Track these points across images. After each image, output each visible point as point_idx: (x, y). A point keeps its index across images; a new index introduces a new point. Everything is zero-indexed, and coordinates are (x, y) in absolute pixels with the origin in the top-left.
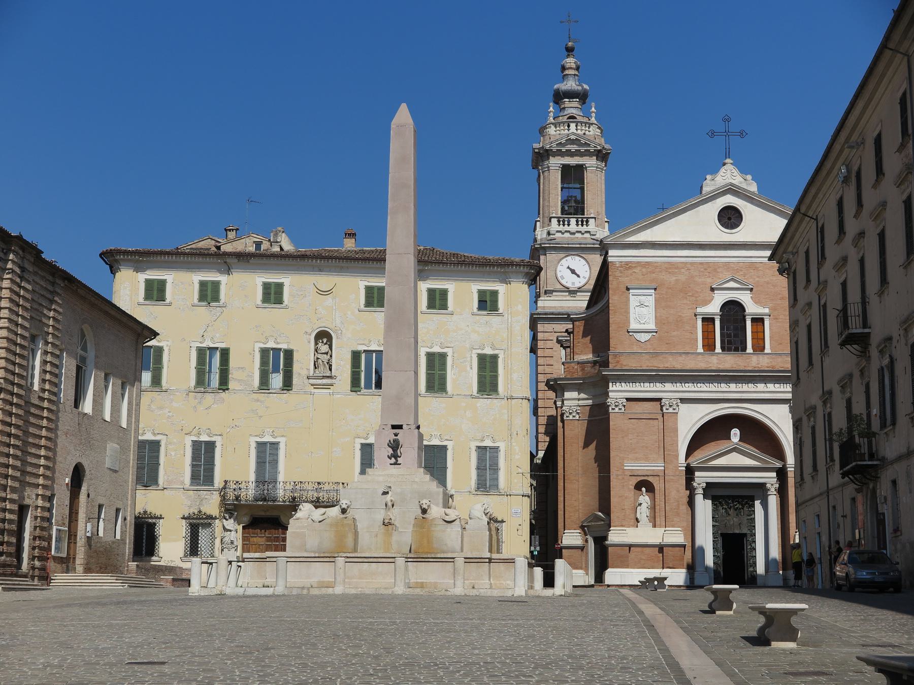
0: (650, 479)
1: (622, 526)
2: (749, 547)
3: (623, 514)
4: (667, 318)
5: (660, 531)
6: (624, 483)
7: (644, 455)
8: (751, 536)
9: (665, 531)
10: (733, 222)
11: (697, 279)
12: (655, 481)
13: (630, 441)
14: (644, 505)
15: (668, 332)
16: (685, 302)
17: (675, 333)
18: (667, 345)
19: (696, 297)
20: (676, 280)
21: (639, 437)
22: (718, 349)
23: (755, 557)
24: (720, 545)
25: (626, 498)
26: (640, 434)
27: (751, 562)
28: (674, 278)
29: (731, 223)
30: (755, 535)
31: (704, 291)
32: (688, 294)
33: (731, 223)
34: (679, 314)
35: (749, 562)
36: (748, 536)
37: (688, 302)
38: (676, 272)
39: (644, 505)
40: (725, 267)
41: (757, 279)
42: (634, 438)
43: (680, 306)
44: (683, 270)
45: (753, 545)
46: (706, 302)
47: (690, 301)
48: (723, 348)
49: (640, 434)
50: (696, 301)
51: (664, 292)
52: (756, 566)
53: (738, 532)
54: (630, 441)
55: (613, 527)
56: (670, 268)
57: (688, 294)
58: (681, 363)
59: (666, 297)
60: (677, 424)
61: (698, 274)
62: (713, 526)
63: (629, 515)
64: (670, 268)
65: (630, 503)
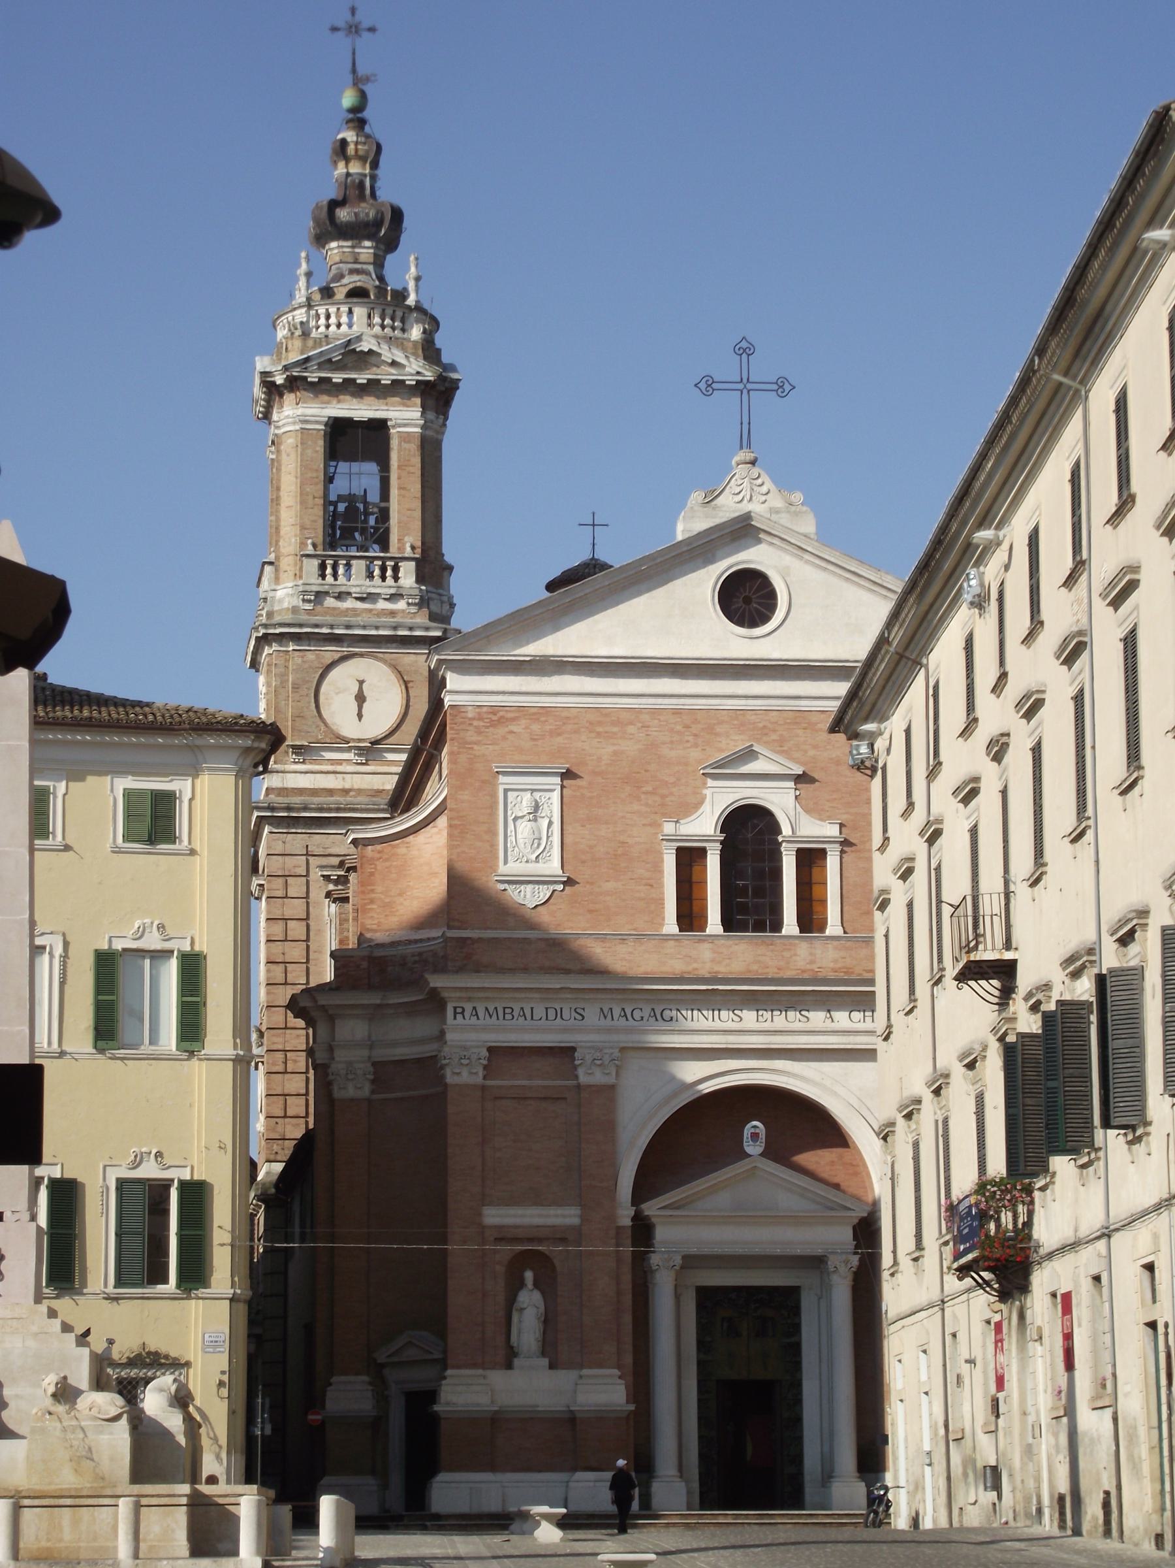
4: (591, 847)
11: (665, 751)
15: (592, 884)
16: (636, 807)
17: (610, 886)
19: (663, 797)
20: (615, 753)
28: (610, 749)
32: (644, 789)
34: (622, 838)
38: (615, 733)
40: (736, 722)
41: (812, 753)
43: (623, 817)
44: (631, 729)
47: (647, 805)
56: (600, 723)
57: (644, 789)
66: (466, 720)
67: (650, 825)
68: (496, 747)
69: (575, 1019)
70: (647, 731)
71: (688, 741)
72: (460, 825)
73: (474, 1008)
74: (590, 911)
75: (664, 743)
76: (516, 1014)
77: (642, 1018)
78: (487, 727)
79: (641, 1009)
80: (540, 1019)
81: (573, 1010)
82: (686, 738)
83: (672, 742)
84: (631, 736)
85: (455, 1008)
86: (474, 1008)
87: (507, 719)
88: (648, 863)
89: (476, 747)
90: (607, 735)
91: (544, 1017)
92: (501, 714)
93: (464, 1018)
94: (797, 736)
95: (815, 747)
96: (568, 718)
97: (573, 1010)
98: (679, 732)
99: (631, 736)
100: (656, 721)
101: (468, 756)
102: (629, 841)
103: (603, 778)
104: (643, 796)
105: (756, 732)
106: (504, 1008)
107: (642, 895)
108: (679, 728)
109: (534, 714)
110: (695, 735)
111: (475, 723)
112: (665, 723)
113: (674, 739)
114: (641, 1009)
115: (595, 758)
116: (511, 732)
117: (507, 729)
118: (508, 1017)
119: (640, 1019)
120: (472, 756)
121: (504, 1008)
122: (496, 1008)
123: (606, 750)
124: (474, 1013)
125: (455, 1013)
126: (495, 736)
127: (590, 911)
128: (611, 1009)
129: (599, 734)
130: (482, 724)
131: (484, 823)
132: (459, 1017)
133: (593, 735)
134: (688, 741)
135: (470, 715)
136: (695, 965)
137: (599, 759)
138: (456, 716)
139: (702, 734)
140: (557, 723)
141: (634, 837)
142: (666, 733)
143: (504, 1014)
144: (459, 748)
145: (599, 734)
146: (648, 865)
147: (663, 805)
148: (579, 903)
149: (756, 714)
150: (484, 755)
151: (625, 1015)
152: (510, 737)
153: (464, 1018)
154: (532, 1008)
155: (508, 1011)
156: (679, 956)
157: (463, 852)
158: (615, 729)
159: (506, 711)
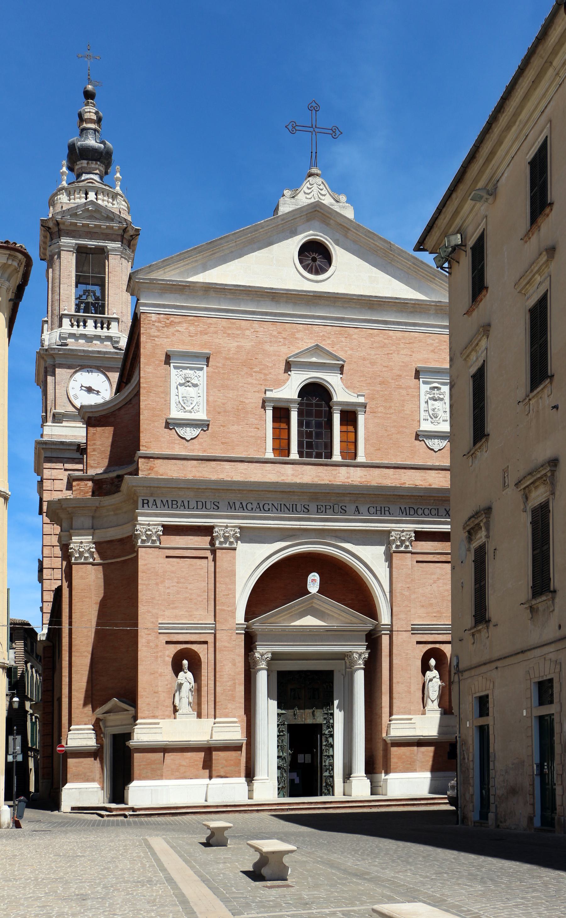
0: (194, 647)
1: (154, 717)
2: (324, 743)
3: (156, 699)
4: (224, 404)
5: (207, 723)
6: (157, 652)
7: (187, 611)
8: (328, 727)
9: (214, 724)
10: (319, 265)
11: (267, 347)
12: (202, 649)
13: (168, 591)
14: (186, 687)
15: (224, 426)
16: (250, 380)
17: (235, 428)
18: (222, 446)
19: (265, 375)
20: (238, 347)
21: (180, 585)
22: (294, 455)
24: (286, 743)
25: (161, 675)
26: (182, 580)
28: (235, 344)
29: (316, 265)
30: (333, 727)
31: (277, 366)
32: (254, 370)
33: (316, 265)
34: (241, 399)
36: (324, 728)
37: (255, 382)
38: (238, 335)
39: (186, 687)
40: (307, 332)
41: (350, 352)
42: (173, 586)
43: (243, 386)
44: (248, 332)
45: (330, 740)
46: (279, 384)
47: (256, 379)
48: (301, 453)
49: (182, 580)
50: (265, 380)
51: (220, 365)
53: (311, 723)
54: (168, 591)
55: (141, 718)
56: (229, 328)
57: (254, 370)
58: (241, 473)
59: (222, 372)
60: (234, 565)
61: (268, 340)
62: (278, 714)
63: (164, 701)
64: (229, 328)
65: (166, 683)
67: (258, 392)
69: (214, 508)
70: (256, 334)
71: (280, 342)
75: (266, 342)
79: (252, 503)
80: (193, 508)
81: (212, 503)
82: (279, 340)
83: (271, 342)
88: (257, 415)
91: (196, 507)
94: (342, 342)
95: (352, 349)
97: (212, 503)
98: (274, 336)
99: (247, 337)
100: (262, 328)
102: (247, 401)
103: (231, 362)
104: (254, 374)
105: (318, 338)
107: (253, 434)
108: (275, 333)
110: (284, 338)
114: (252, 503)
115: (226, 349)
123: (233, 344)
128: (234, 503)
129: (229, 334)
134: (280, 342)
136: (283, 478)
137: (229, 350)
141: (248, 399)
142: (268, 336)
146: (256, 416)
147: (265, 380)
148: (217, 438)
149: (319, 327)
151: (243, 507)
154: (188, 501)
156: (273, 472)
158: (239, 332)
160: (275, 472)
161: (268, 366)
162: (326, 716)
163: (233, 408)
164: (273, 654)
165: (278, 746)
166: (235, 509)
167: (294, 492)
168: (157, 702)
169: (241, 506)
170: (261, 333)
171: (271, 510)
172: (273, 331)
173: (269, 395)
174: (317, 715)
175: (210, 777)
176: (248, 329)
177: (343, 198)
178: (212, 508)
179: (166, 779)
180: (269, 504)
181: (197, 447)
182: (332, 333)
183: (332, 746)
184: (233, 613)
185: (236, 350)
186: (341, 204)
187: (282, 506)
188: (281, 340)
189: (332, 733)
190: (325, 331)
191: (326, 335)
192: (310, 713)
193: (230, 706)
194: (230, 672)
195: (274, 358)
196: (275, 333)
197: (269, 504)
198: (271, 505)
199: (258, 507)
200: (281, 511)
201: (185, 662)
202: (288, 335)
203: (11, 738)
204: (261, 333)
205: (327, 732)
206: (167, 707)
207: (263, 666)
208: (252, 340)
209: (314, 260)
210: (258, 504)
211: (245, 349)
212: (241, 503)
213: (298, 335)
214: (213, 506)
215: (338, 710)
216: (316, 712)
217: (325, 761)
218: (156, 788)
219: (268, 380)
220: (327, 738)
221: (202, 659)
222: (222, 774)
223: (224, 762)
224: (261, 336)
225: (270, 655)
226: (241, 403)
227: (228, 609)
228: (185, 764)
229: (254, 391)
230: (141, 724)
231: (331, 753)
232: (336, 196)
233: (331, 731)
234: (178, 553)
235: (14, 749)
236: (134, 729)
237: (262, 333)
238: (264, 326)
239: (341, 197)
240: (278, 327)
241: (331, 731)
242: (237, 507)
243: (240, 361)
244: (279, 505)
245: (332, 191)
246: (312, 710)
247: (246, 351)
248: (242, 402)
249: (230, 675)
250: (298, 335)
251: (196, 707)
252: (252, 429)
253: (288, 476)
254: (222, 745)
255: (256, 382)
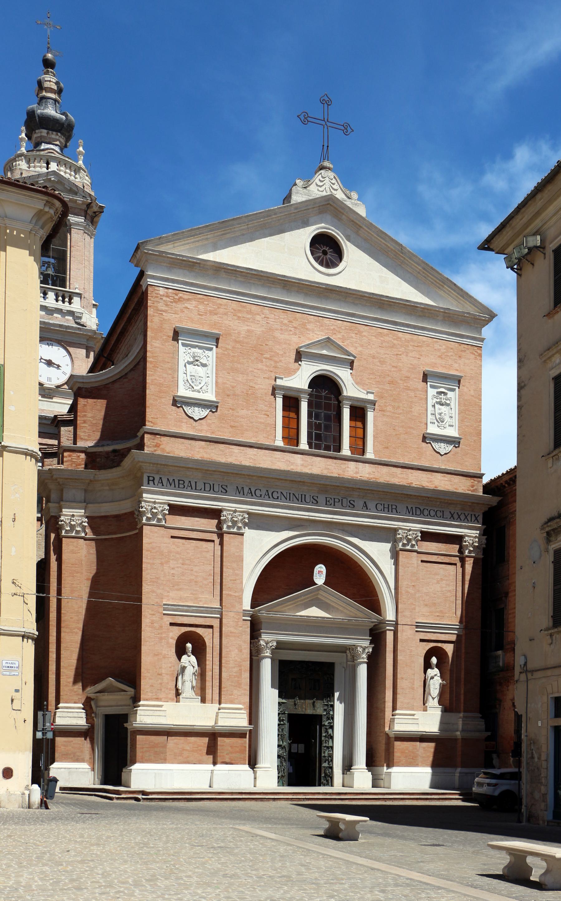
0: (199, 631)
1: (158, 699)
2: (324, 734)
3: (160, 681)
4: (233, 387)
5: (212, 708)
6: (162, 633)
7: (192, 594)
8: (328, 719)
9: (219, 709)
10: (330, 259)
11: (277, 334)
12: (207, 633)
13: (172, 572)
14: (189, 671)
15: (233, 410)
16: (260, 366)
17: (244, 412)
18: (231, 429)
19: (276, 362)
20: (248, 331)
21: (186, 566)
22: (304, 445)
23: (332, 747)
24: (286, 732)
25: (164, 657)
26: (187, 562)
27: (326, 754)
28: (246, 328)
29: (326, 258)
30: (333, 718)
31: (287, 354)
32: (265, 356)
33: (326, 258)
34: (251, 384)
35: (323, 755)
36: (324, 719)
37: (265, 368)
38: (249, 319)
39: (189, 671)
40: (318, 324)
42: (178, 567)
43: (252, 371)
44: (258, 318)
45: (330, 731)
46: (290, 373)
47: (267, 366)
48: (310, 444)
49: (187, 562)
50: (275, 367)
51: (230, 347)
52: (332, 761)
53: (311, 713)
54: (172, 572)
55: (144, 700)
56: (239, 311)
57: (265, 356)
58: (250, 458)
59: (232, 354)
60: (242, 550)
61: (279, 328)
62: (279, 703)
63: (168, 683)
64: (239, 311)
65: (170, 665)
66: (159, 295)
67: (268, 378)
68: (176, 316)
69: (222, 492)
70: (267, 320)
71: (291, 331)
72: (153, 362)
73: (161, 478)
74: (232, 427)
75: (277, 330)
76: (186, 485)
77: (261, 495)
78: (171, 302)
79: (260, 490)
80: (201, 490)
81: (220, 486)
82: (290, 328)
83: (281, 329)
84: (258, 322)
85: (149, 477)
86: (161, 478)
87: (184, 299)
88: (267, 402)
89: (164, 313)
90: (243, 319)
91: (203, 489)
92: (181, 295)
93: (154, 484)
96: (221, 305)
97: (220, 486)
98: (285, 324)
99: (258, 322)
100: (273, 315)
101: (160, 319)
102: (257, 387)
103: (241, 345)
104: (264, 360)
105: (329, 332)
106: (179, 480)
107: (262, 421)
108: (286, 321)
109: (200, 299)
110: (295, 328)
111: (164, 298)
112: (278, 317)
113: (283, 328)
114: (260, 490)
115: (236, 332)
116: (186, 308)
117: (183, 306)
118: (181, 486)
119: (259, 496)
120: (162, 319)
121: (179, 480)
122: (174, 480)
123: (243, 328)
124: (160, 481)
125: (149, 480)
126: (176, 309)
127: (232, 427)
128: (243, 488)
129: (239, 317)
130: (168, 299)
131: (168, 362)
132: (151, 483)
133: (235, 318)
134: (291, 331)
135: (161, 293)
136: (292, 467)
137: (239, 333)
138: (152, 292)
139: (299, 327)
140: (214, 307)
141: (258, 384)
142: (278, 323)
143: (179, 484)
144: (154, 313)
145: (239, 318)
146: (266, 403)
147: (275, 367)
148: (225, 421)
149: (330, 321)
150: (169, 320)
151: (251, 492)
152: (185, 310)
153: (154, 484)
154: (196, 482)
155: (181, 482)
156: (282, 460)
157: (155, 379)
158: (249, 316)
159: (184, 294)
160: (284, 461)
161: (278, 353)
162: (326, 708)
163: (243, 392)
164: (278, 642)
165: (278, 735)
166: (244, 495)
167: (304, 482)
168: (161, 684)
169: (249, 492)
170: (271, 320)
171: (279, 498)
172: (284, 319)
173: (279, 382)
174: (318, 706)
175: (215, 763)
176: (258, 314)
177: (355, 195)
178: (220, 491)
179: (169, 763)
180: (278, 492)
181: (205, 427)
182: (342, 328)
183: (332, 737)
184: (240, 599)
185: (247, 334)
186: (353, 201)
187: (291, 495)
188: (292, 329)
189: (332, 724)
190: (335, 325)
191: (337, 329)
192: (310, 703)
193: (235, 692)
194: (236, 658)
195: (284, 346)
196: (286, 321)
197: (278, 492)
198: (279, 493)
199: (267, 494)
200: (290, 500)
201: (189, 645)
202: (299, 324)
203: (40, 714)
204: (271, 320)
205: (326, 723)
206: (170, 689)
207: (268, 654)
208: (263, 326)
209: (325, 253)
210: (267, 491)
211: (256, 334)
212: (250, 489)
213: (309, 326)
214: (221, 488)
215: (339, 702)
216: (317, 703)
217: (324, 752)
218: (160, 771)
219: (278, 368)
220: (327, 729)
221: (207, 643)
222: (227, 760)
223: (230, 748)
224: (271, 323)
225: (275, 644)
226: (251, 388)
227: (234, 594)
228: (188, 748)
229: (264, 378)
230: (143, 705)
231: (330, 744)
232: (348, 192)
233: (331, 723)
234: (184, 534)
235: (44, 725)
236: (137, 710)
237: (273, 320)
238: (275, 313)
239: (352, 194)
240: (289, 316)
241: (331, 723)
242: (246, 492)
243: (250, 345)
244: (288, 495)
245: (344, 187)
246: (312, 701)
247: (257, 336)
248: (252, 387)
249: (236, 661)
250: (309, 326)
251: (199, 691)
252: (262, 416)
253: (297, 466)
254: (227, 732)
255: (266, 368)
